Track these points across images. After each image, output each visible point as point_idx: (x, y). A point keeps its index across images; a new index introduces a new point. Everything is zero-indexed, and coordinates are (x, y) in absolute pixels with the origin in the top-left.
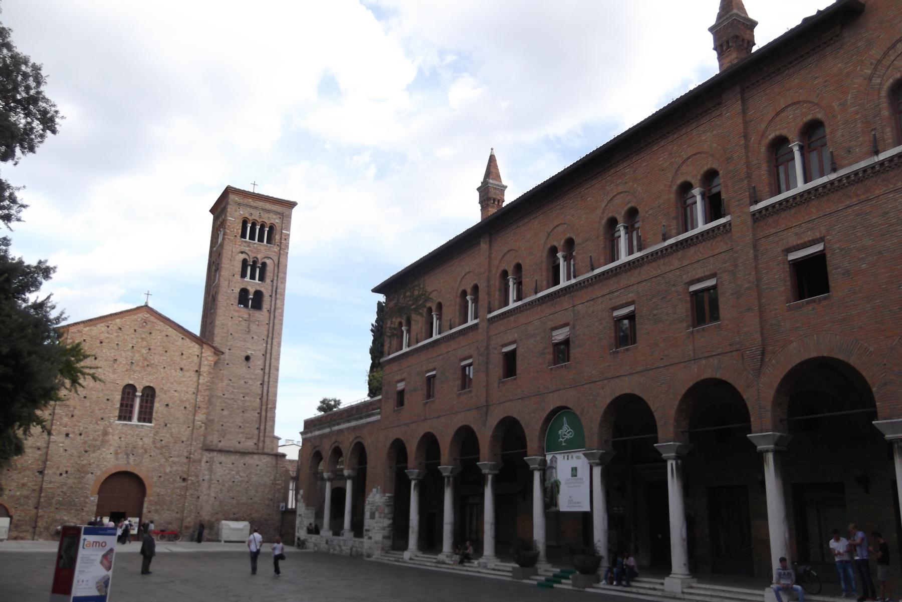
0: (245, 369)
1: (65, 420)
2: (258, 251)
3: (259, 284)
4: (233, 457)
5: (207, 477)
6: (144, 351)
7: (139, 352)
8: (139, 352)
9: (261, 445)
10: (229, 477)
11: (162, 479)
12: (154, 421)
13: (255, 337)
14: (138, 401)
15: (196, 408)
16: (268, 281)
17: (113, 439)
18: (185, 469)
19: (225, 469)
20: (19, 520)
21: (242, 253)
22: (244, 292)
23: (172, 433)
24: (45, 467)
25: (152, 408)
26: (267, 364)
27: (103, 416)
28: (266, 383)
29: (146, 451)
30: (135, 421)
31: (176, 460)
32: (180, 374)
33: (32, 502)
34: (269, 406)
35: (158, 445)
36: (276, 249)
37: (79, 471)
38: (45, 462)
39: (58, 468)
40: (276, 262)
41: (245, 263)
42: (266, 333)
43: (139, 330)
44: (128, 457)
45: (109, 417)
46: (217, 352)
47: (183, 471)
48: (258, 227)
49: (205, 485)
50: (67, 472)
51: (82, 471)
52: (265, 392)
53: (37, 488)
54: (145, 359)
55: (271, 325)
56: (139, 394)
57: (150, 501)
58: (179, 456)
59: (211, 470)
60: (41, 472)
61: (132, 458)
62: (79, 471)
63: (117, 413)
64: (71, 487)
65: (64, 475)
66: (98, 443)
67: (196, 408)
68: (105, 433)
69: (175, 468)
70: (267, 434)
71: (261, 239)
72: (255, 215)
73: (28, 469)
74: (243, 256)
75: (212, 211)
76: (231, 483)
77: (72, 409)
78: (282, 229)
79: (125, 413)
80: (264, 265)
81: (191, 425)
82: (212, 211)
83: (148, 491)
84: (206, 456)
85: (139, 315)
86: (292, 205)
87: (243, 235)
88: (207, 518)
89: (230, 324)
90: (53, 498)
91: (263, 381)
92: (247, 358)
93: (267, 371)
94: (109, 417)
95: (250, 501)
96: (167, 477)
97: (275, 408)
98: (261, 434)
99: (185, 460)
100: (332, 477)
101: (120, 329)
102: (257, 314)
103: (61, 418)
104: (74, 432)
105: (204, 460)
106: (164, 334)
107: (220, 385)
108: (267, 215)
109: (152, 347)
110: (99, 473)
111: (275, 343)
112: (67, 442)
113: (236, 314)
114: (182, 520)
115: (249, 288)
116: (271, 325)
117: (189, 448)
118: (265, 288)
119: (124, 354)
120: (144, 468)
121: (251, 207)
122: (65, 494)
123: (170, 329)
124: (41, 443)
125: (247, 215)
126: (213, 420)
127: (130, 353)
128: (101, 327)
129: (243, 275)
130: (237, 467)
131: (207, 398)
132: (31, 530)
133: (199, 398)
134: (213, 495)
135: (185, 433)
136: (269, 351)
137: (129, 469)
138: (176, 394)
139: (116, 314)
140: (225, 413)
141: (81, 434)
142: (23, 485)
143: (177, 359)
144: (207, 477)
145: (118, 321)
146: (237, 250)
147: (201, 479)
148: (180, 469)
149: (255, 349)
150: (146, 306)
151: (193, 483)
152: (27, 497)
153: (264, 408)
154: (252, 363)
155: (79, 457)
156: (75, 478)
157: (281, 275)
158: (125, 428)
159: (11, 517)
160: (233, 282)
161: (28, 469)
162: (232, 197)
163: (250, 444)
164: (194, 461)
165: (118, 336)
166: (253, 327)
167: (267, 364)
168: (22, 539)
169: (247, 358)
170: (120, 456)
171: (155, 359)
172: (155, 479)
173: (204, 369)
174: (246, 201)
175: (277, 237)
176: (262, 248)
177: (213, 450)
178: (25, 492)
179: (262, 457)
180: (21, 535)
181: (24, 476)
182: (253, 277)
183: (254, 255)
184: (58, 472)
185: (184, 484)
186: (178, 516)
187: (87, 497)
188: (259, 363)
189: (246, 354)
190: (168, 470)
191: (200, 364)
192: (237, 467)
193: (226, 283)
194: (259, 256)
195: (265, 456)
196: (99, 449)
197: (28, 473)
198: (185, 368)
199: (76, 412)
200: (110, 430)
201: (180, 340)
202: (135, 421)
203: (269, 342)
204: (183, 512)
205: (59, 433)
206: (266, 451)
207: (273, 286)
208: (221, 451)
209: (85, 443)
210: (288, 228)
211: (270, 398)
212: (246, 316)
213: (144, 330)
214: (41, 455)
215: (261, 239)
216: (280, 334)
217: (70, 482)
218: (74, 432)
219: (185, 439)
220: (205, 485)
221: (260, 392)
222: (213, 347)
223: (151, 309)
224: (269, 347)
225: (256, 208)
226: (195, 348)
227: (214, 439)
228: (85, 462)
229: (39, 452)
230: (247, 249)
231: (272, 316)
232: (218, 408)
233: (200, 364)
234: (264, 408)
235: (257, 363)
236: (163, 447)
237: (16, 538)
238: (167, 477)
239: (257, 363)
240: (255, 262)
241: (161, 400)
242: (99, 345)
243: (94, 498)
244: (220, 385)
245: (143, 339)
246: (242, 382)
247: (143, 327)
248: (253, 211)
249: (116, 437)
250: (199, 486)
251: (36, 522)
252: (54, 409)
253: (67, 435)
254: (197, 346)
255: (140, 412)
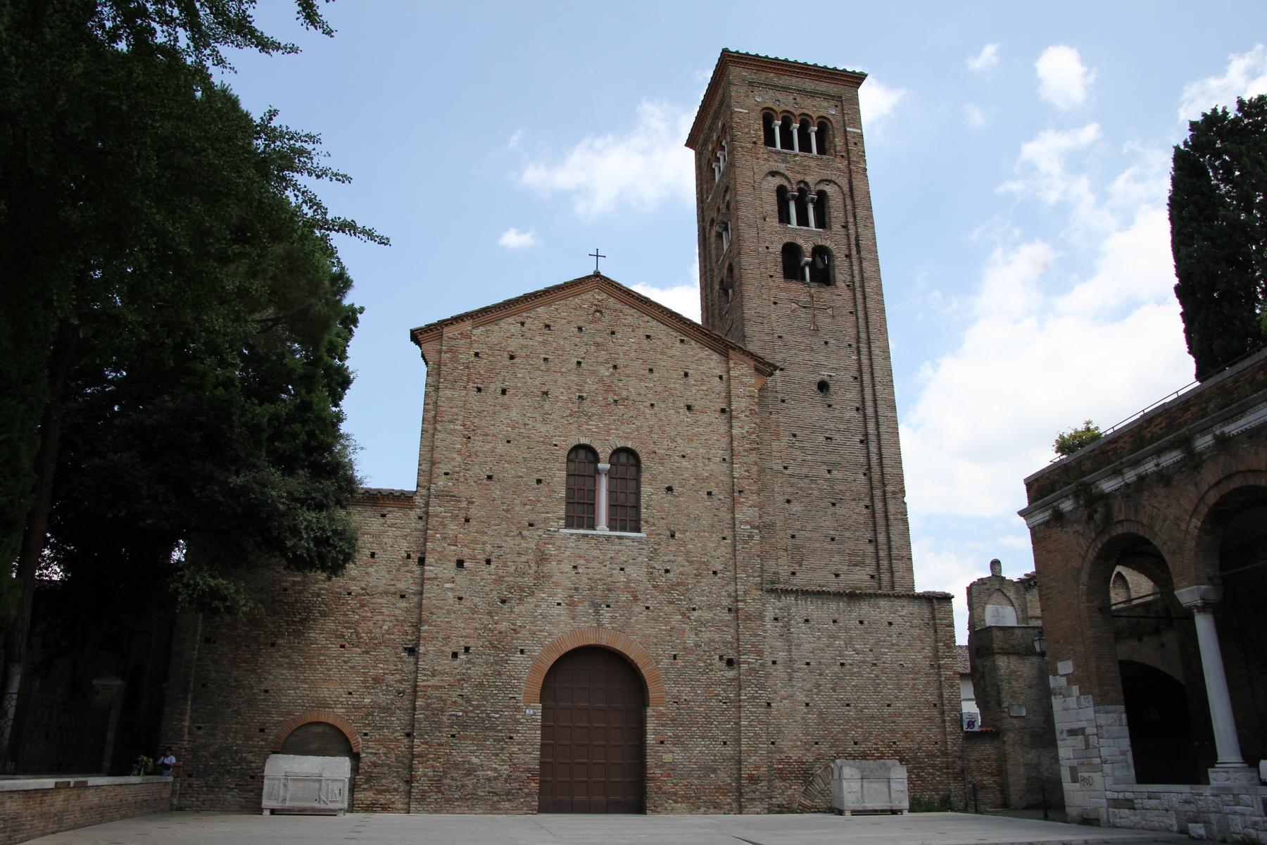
0: (820, 410)
1: (453, 528)
2: (806, 169)
3: (819, 235)
4: (833, 606)
5: (781, 656)
6: (605, 371)
7: (593, 373)
8: (593, 373)
9: (885, 577)
10: (830, 652)
11: (680, 662)
12: (644, 527)
13: (832, 341)
14: (603, 484)
15: (735, 493)
16: (837, 227)
17: (560, 570)
18: (729, 638)
19: (817, 632)
20: (375, 765)
21: (773, 174)
22: (791, 252)
23: (688, 552)
24: (419, 638)
25: (638, 493)
26: (868, 397)
27: (532, 517)
28: (872, 438)
29: (636, 598)
30: (602, 528)
31: (707, 615)
32: (688, 418)
33: (398, 720)
34: (889, 488)
35: (662, 582)
36: (841, 164)
37: (494, 647)
38: (417, 626)
39: (447, 638)
40: (846, 189)
41: (781, 192)
42: (852, 332)
43: (586, 327)
44: (597, 612)
45: (546, 520)
46: (765, 368)
47: (725, 643)
48: (796, 126)
49: (780, 672)
50: (467, 649)
51: (500, 646)
52: (874, 458)
53: (405, 686)
54: (609, 389)
55: (861, 314)
56: (604, 466)
57: (660, 716)
58: (710, 607)
59: (786, 636)
60: (412, 651)
61: (606, 614)
62: (494, 647)
63: (562, 513)
64: (481, 684)
65: (462, 657)
66: (528, 581)
67: (735, 493)
68: (543, 559)
69: (706, 636)
70: (894, 552)
71: (805, 147)
72: (785, 103)
73: (384, 643)
74: (777, 181)
75: (689, 144)
76: (836, 669)
77: (464, 504)
78: (845, 126)
79: (580, 512)
80: (822, 195)
81: (727, 533)
82: (689, 144)
83: (653, 694)
84: (773, 607)
85: (584, 297)
86: (858, 79)
87: (770, 141)
88: (795, 755)
89: (773, 317)
90: (442, 710)
91: (866, 434)
92: (823, 386)
93: (870, 411)
94: (546, 520)
95: (886, 710)
96: (692, 658)
97: (903, 491)
98: (882, 554)
99: (728, 617)
100: (1212, 597)
101: (548, 326)
102: (826, 294)
103: (445, 526)
104: (474, 558)
105: (769, 615)
106: (641, 333)
107: (775, 445)
108: (808, 102)
109: (620, 362)
110: (537, 651)
111: (876, 351)
112: (462, 578)
113: (784, 295)
114: (739, 762)
115: (800, 242)
116: (861, 314)
117: (731, 588)
118: (834, 241)
119: (561, 380)
120: (636, 638)
121: (774, 87)
122: (469, 701)
123: (654, 323)
124: (406, 583)
125: (770, 105)
126: (772, 525)
127: (574, 378)
128: (509, 325)
129: (784, 218)
130: (847, 630)
131: (755, 469)
132: (403, 787)
133: (739, 471)
134: (801, 697)
135: (719, 555)
136: (866, 369)
137: (604, 640)
138: (685, 463)
139: (536, 295)
140: (795, 507)
141: (488, 562)
142: (377, 680)
143: (677, 385)
144: (781, 656)
145: (540, 310)
146: (759, 174)
147: (769, 660)
148: (717, 637)
149: (838, 366)
150: (597, 275)
151: (752, 670)
152: (386, 709)
153: (878, 493)
154: (833, 399)
155: (490, 613)
156: (486, 663)
157: (861, 213)
158: (583, 544)
159: (355, 757)
160: (761, 237)
161: (384, 643)
162: (735, 72)
163: (860, 577)
164: (748, 618)
165: (544, 343)
166: (823, 320)
167: (868, 397)
168: (385, 808)
169: (823, 386)
170: (580, 608)
171: (631, 388)
172: (665, 662)
173: (739, 405)
174: (763, 77)
175: (839, 141)
176: (813, 164)
177: (787, 592)
178: (383, 699)
179: (897, 603)
180: (382, 799)
181: (378, 661)
182: (803, 221)
183: (800, 177)
184: (449, 650)
185: (731, 674)
186: (728, 751)
187: (517, 709)
188: (849, 396)
189: (818, 379)
190: (690, 640)
191: (729, 395)
192: (847, 630)
193: (753, 232)
194: (808, 179)
195: (904, 602)
196: (532, 594)
197: (385, 651)
198: (698, 405)
199: (473, 512)
200: (551, 549)
201: (678, 344)
202: (602, 528)
203: (864, 350)
204: (738, 741)
205: (442, 558)
206: (898, 589)
207: (848, 236)
208: (805, 593)
209: (500, 580)
210: (857, 122)
211: (887, 470)
212: (804, 298)
213: (600, 326)
214: (408, 610)
215: (805, 147)
216: (883, 331)
217: (476, 672)
218: (474, 558)
219: (719, 567)
220: (780, 672)
221: (863, 460)
222: (752, 355)
223: (606, 279)
224: (865, 361)
225: (785, 89)
226: (712, 362)
227: (782, 566)
228: (504, 626)
229: (403, 604)
230: (781, 167)
231: (859, 295)
232: (780, 499)
233: (729, 395)
234: (878, 493)
235: (846, 395)
236: (672, 587)
237: (370, 808)
238: (692, 658)
239: (846, 395)
240: (803, 192)
241: (654, 478)
242: (508, 363)
243: (534, 711)
244: (775, 445)
245: (597, 344)
246: (821, 438)
247: (598, 321)
248: (779, 95)
249: (567, 567)
250: (767, 676)
251: (411, 768)
252: (427, 504)
253: (460, 563)
254: (715, 356)
255: (612, 506)
